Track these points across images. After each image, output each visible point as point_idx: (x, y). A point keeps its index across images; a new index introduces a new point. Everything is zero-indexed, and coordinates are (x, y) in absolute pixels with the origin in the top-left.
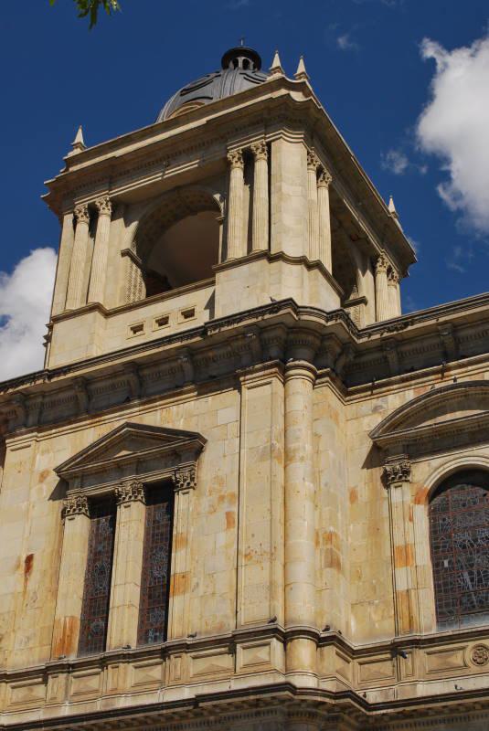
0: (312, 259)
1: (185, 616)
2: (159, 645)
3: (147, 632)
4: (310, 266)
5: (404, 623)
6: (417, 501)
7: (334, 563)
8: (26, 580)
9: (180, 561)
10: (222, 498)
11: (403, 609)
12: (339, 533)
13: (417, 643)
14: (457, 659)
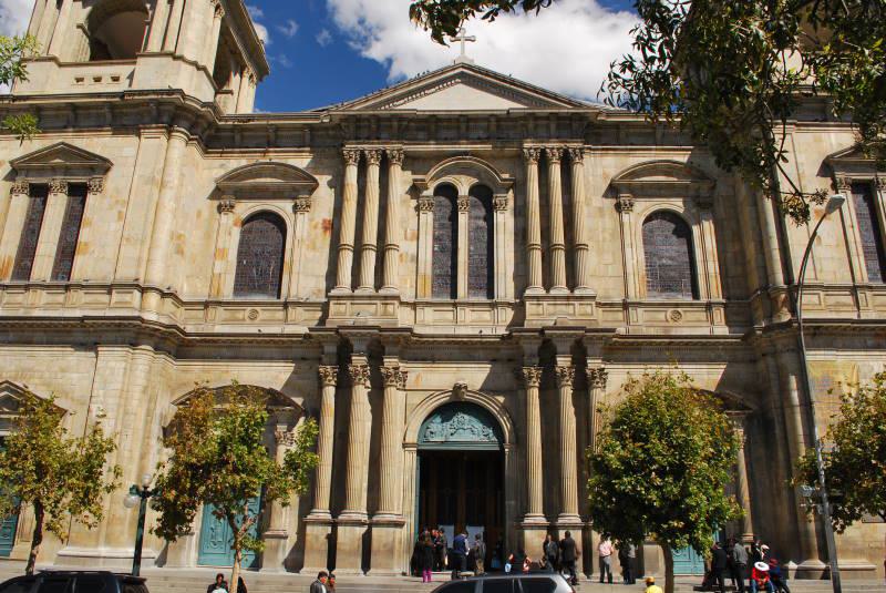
0: (201, 63)
1: (83, 268)
2: (64, 283)
3: (58, 273)
4: (199, 68)
5: (214, 292)
6: (235, 225)
7: (180, 252)
9: (85, 235)
10: (117, 202)
11: (215, 283)
12: (187, 236)
13: (220, 303)
14: (240, 315)
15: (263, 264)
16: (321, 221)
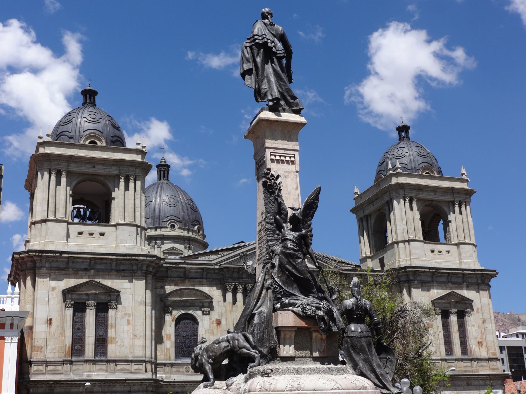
6: (173, 321)
8: (50, 328)
9: (111, 333)
14: (181, 370)
15: (187, 341)
16: (215, 320)
